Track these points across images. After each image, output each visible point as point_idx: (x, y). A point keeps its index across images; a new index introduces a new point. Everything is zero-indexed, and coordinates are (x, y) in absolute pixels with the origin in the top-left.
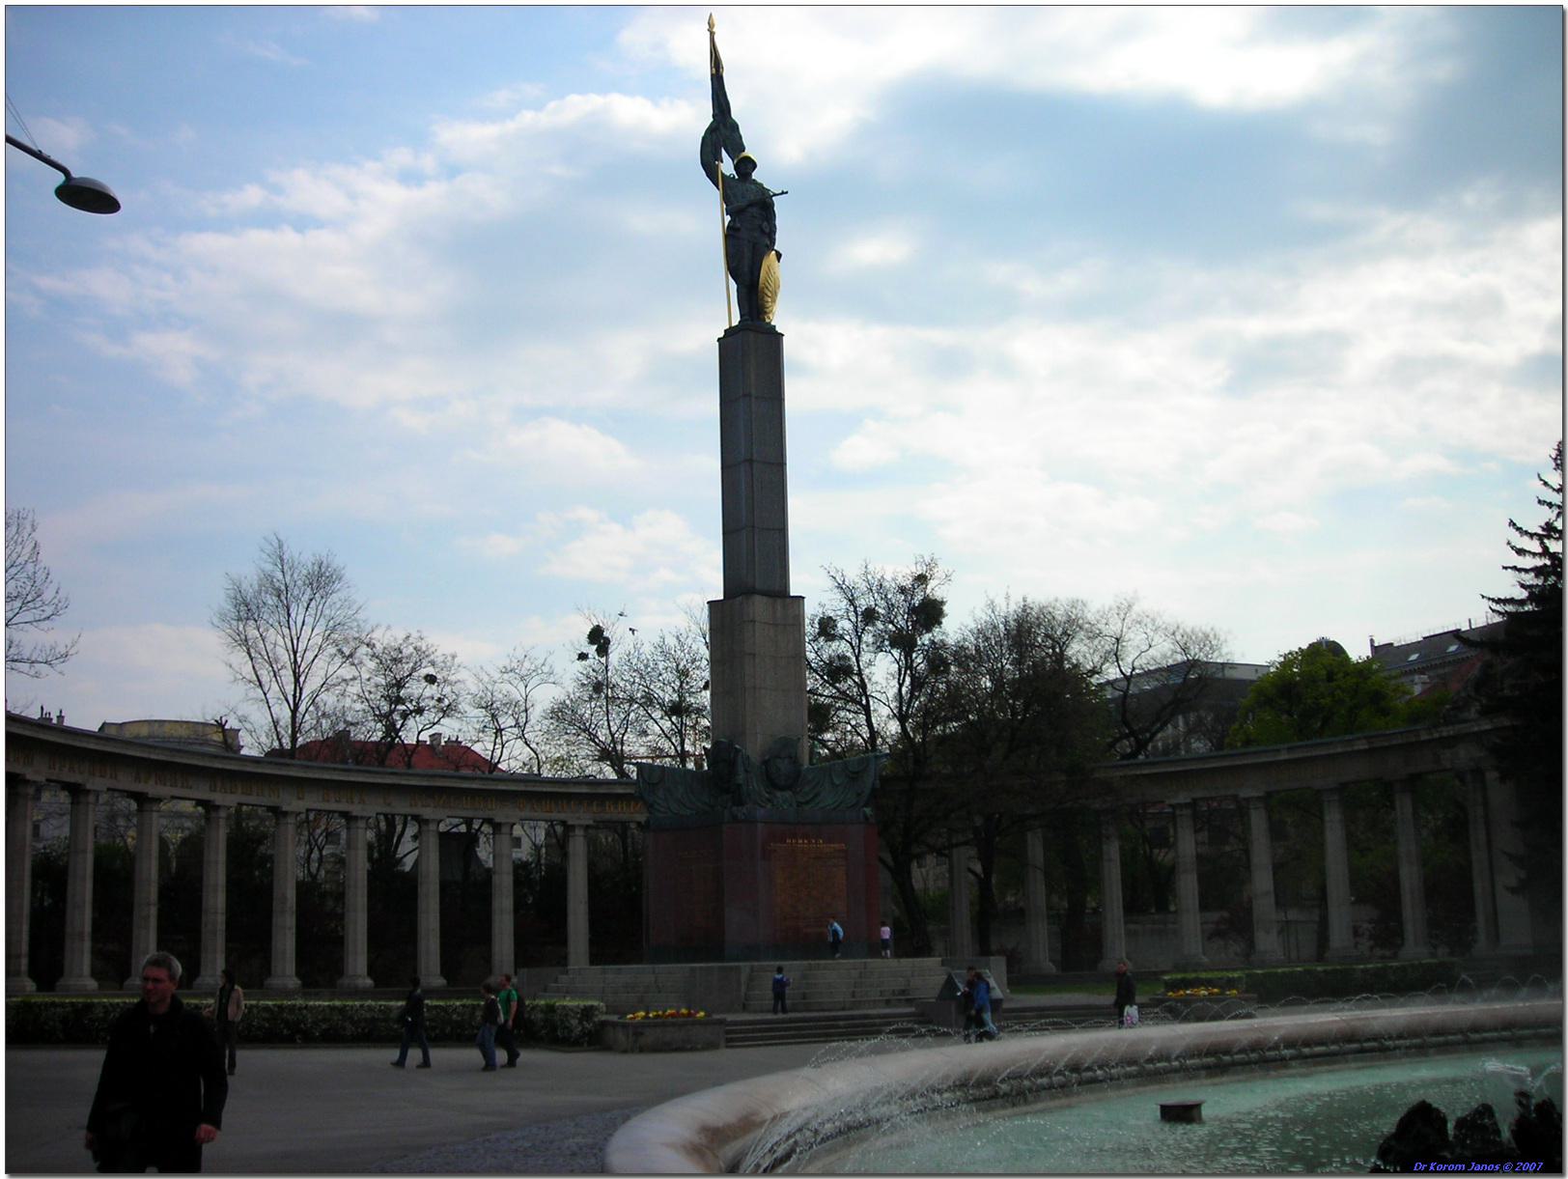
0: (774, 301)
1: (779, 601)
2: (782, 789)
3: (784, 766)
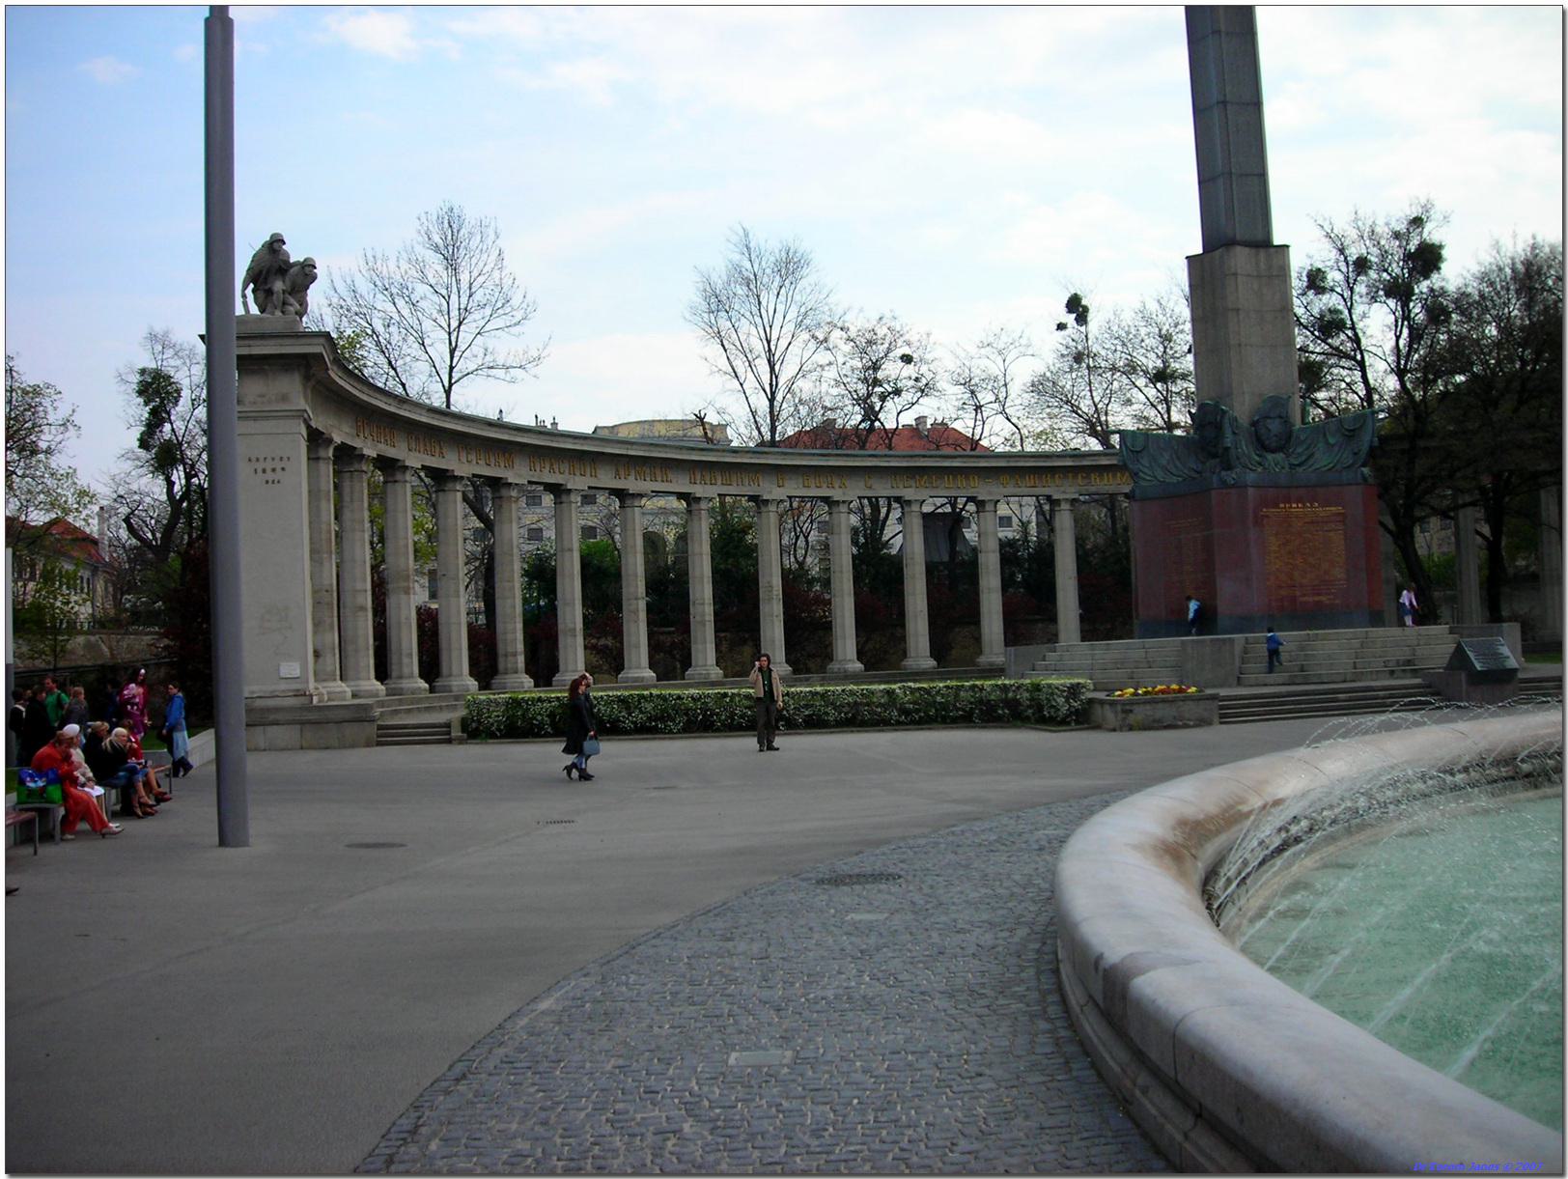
2: (1273, 451)
3: (1275, 426)
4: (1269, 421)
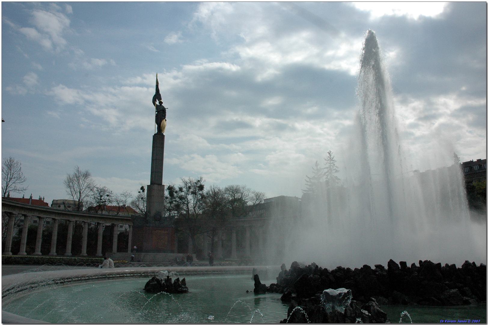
0: (164, 129)
1: (160, 186)
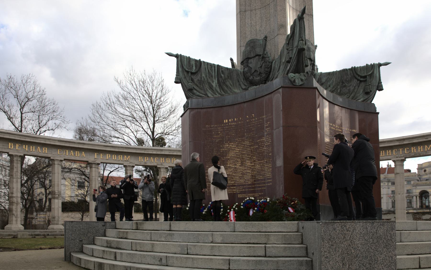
4: (250, 61)
